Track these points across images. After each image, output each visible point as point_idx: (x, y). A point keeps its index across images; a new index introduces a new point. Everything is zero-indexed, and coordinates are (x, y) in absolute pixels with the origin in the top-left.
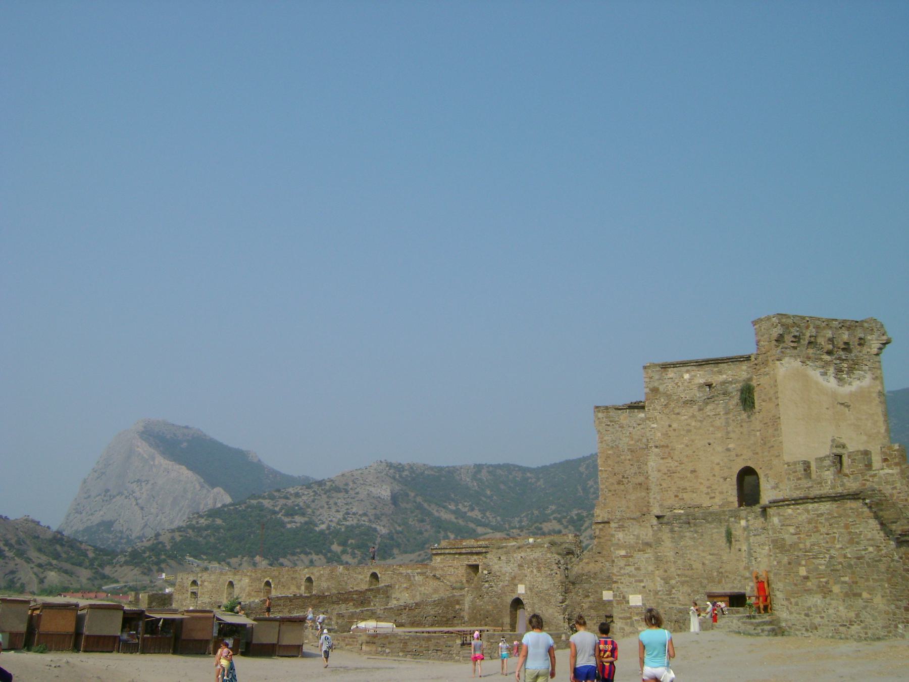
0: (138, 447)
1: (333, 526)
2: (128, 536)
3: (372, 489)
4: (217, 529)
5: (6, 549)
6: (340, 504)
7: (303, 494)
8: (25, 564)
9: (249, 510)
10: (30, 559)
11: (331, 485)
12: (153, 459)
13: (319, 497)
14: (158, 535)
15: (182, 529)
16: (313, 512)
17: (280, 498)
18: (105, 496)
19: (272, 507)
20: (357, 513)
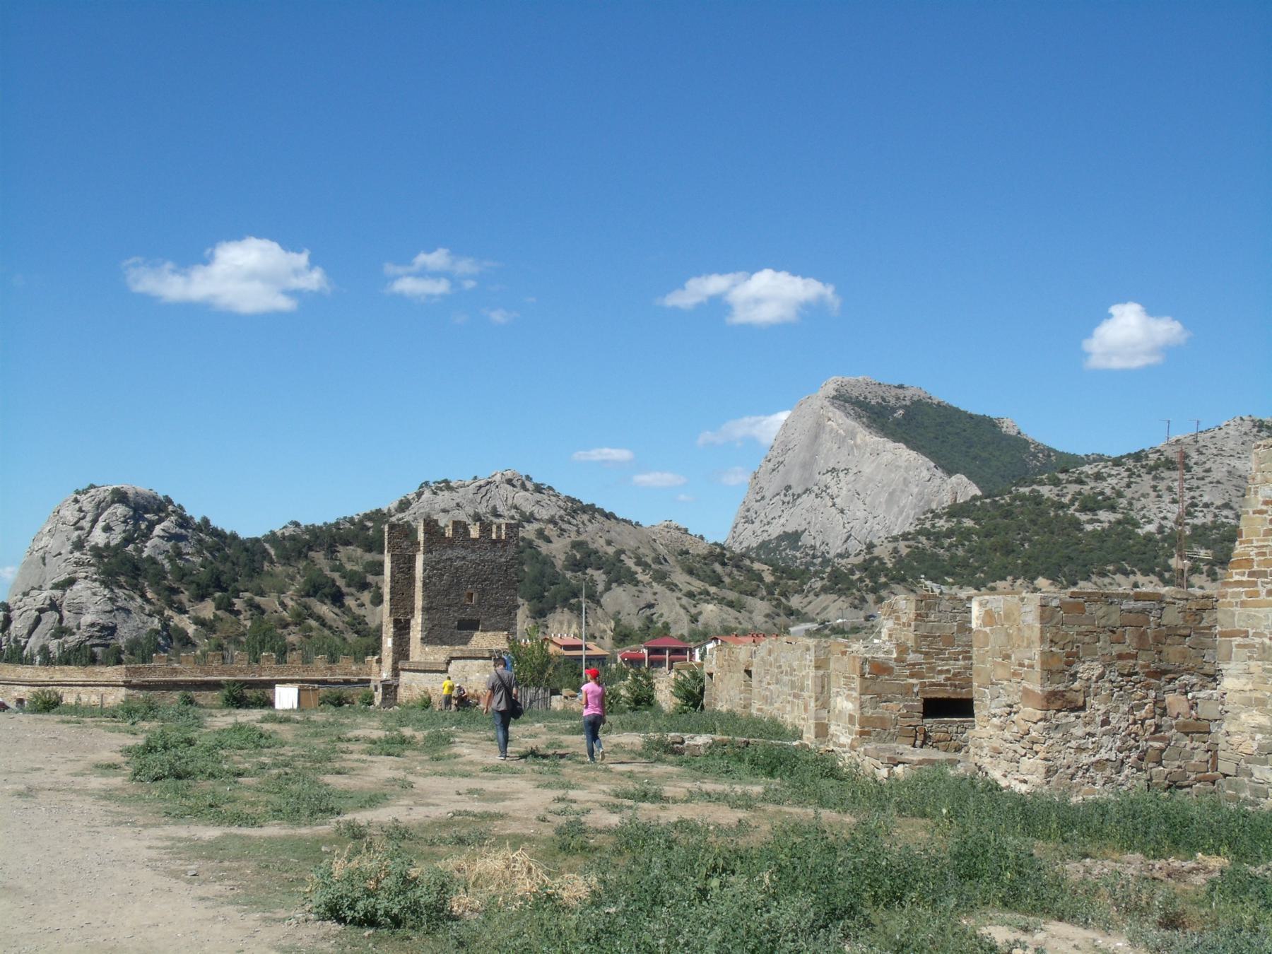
0: (829, 419)
1: (1168, 526)
2: (823, 553)
3: (1234, 462)
4: (967, 534)
5: (639, 569)
6: (1177, 490)
7: (1110, 475)
8: (668, 593)
9: (1018, 503)
10: (676, 585)
11: (1159, 459)
12: (853, 437)
13: (1138, 480)
14: (870, 546)
15: (910, 536)
16: (1130, 504)
17: (1070, 482)
18: (785, 495)
19: (1057, 498)
20: (1212, 504)
